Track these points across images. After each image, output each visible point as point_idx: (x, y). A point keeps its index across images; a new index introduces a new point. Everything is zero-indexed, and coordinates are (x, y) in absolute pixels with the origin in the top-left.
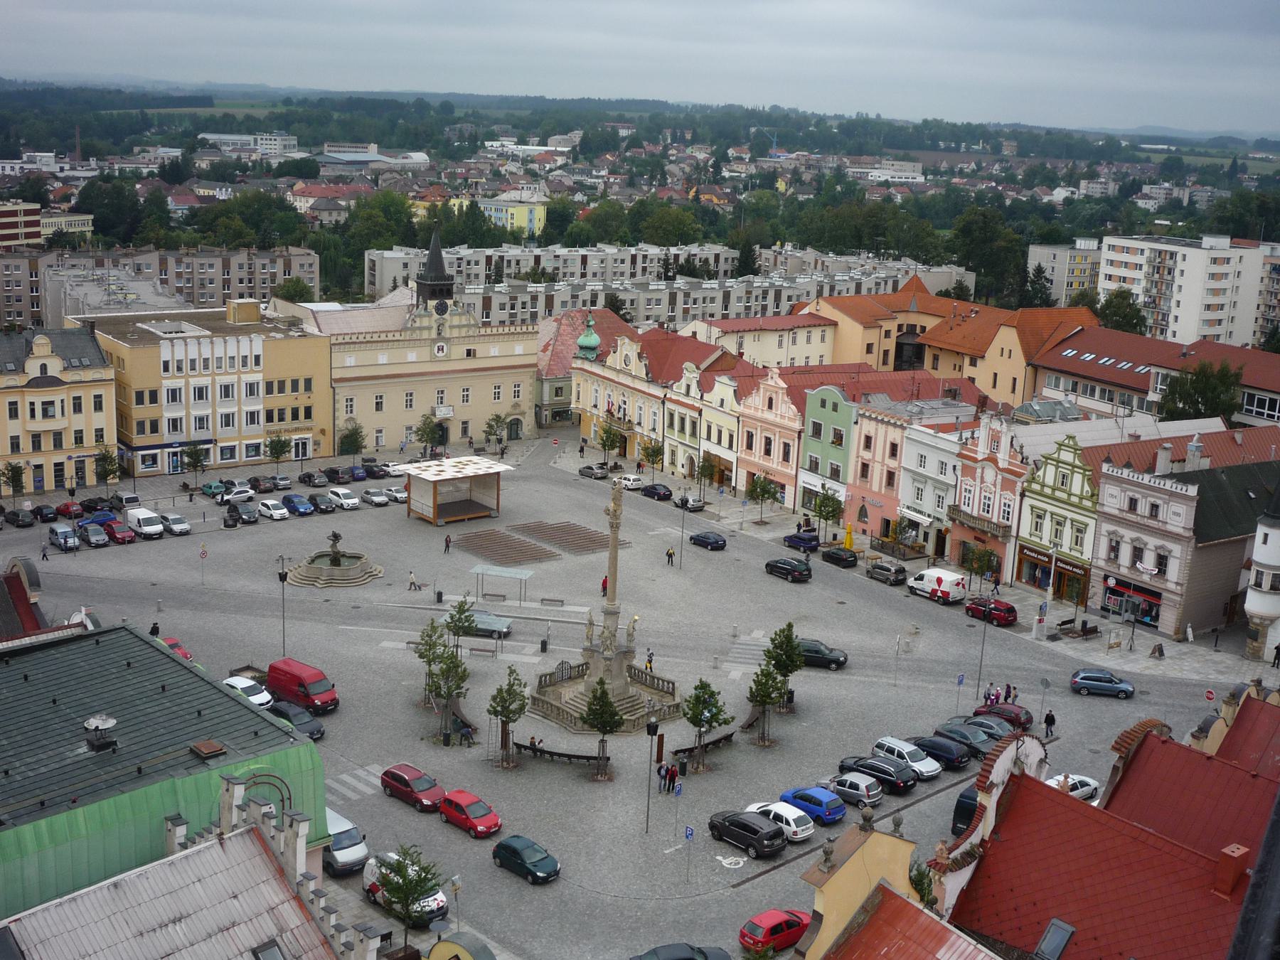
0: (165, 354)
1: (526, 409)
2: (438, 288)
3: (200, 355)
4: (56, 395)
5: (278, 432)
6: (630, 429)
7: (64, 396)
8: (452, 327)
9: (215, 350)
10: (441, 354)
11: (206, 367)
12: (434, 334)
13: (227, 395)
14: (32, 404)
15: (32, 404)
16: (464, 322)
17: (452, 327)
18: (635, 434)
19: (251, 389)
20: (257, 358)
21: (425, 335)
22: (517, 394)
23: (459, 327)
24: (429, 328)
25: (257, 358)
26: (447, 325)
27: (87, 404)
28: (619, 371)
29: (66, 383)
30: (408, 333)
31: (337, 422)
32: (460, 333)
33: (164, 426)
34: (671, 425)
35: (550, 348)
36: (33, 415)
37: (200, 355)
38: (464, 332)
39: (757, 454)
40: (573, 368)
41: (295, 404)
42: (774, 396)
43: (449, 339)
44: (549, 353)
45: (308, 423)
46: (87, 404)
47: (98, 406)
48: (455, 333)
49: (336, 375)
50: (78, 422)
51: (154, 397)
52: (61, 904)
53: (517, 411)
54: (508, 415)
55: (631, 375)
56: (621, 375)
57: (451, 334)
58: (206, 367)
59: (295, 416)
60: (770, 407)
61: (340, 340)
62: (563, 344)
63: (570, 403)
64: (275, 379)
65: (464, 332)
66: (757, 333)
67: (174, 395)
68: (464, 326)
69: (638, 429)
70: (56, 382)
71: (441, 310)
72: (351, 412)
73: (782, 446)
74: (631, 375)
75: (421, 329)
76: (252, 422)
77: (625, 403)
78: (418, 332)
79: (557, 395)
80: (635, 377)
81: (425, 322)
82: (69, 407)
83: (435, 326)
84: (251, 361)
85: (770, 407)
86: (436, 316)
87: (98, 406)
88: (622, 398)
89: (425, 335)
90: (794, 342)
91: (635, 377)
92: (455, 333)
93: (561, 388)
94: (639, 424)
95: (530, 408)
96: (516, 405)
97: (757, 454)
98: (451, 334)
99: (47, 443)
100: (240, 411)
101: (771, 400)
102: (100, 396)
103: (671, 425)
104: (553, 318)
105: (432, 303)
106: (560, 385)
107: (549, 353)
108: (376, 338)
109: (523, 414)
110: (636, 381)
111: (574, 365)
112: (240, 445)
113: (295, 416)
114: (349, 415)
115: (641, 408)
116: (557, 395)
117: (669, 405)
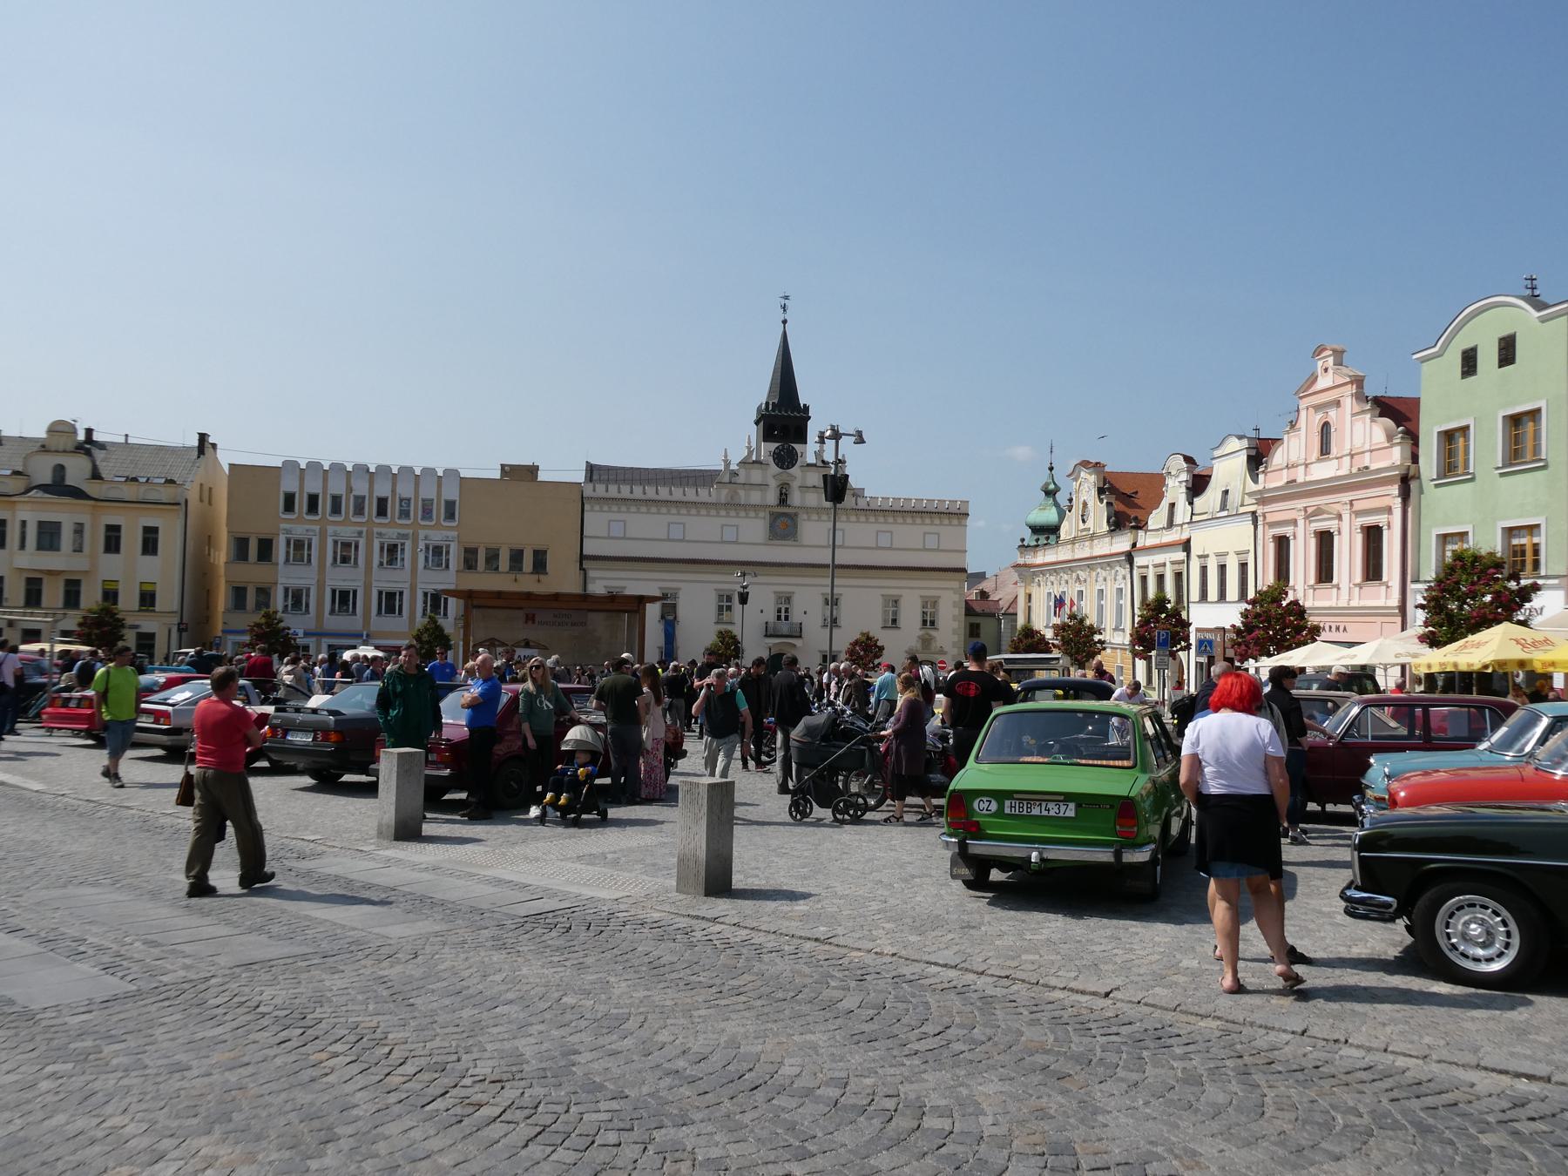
0: (289, 484)
3: (350, 489)
4: (65, 514)
7: (85, 519)
9: (376, 487)
11: (359, 510)
12: (772, 498)
13: (392, 561)
14: (24, 523)
15: (24, 523)
19: (437, 553)
20: (450, 506)
22: (929, 622)
24: (763, 486)
25: (450, 506)
26: (795, 485)
27: (132, 539)
29: (88, 497)
33: (278, 601)
36: (22, 546)
37: (350, 489)
46: (132, 539)
47: (150, 543)
50: (111, 567)
51: (266, 549)
58: (359, 510)
64: (482, 540)
67: (299, 548)
70: (77, 493)
71: (786, 459)
75: (748, 485)
77: (1081, 593)
81: (756, 476)
82: (95, 539)
83: (773, 484)
84: (439, 511)
87: (150, 543)
89: (755, 497)
95: (954, 645)
99: (53, 594)
102: (155, 530)
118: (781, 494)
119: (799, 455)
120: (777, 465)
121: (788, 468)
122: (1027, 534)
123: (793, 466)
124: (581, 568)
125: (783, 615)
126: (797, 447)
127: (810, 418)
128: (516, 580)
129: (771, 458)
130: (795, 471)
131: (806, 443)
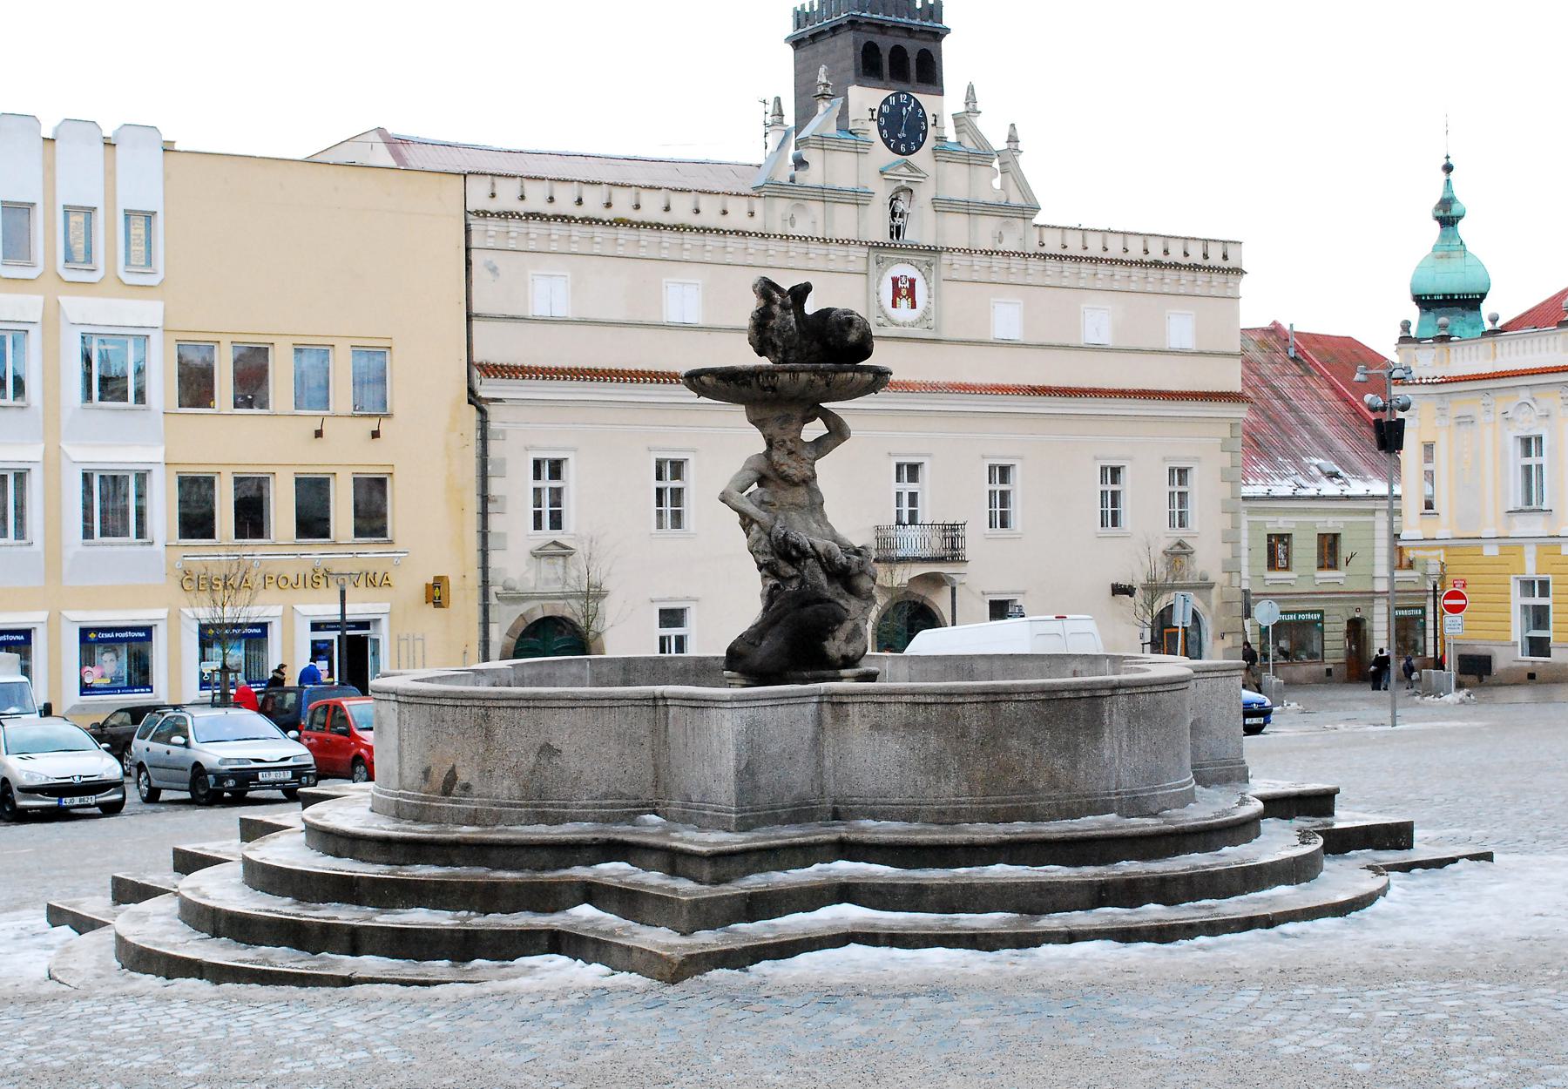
2: (885, 43)
5: (228, 584)
8: (942, 206)
10: (903, 312)
17: (942, 206)
21: (844, 221)
24: (859, 198)
26: (924, 194)
30: (782, 206)
31: (495, 559)
41: (315, 460)
43: (934, 251)
45: (371, 552)
48: (955, 230)
49: (493, 345)
59: (312, 523)
61: (507, 198)
68: (989, 209)
72: (556, 522)
75: (827, 195)
76: (113, 525)
78: (816, 208)
83: (883, 192)
86: (882, 154)
92: (955, 230)
96: (1179, 553)
100: (53, 461)
105: (866, 99)
108: (652, 209)
112: (53, 623)
113: (312, 523)
114: (547, 534)
118: (894, 214)
119: (930, 120)
120: (887, 142)
121: (910, 152)
122: (1413, 313)
123: (919, 145)
124: (473, 397)
125: (906, 508)
126: (925, 100)
127: (948, 30)
128: (319, 434)
129: (874, 126)
130: (922, 158)
131: (941, 93)
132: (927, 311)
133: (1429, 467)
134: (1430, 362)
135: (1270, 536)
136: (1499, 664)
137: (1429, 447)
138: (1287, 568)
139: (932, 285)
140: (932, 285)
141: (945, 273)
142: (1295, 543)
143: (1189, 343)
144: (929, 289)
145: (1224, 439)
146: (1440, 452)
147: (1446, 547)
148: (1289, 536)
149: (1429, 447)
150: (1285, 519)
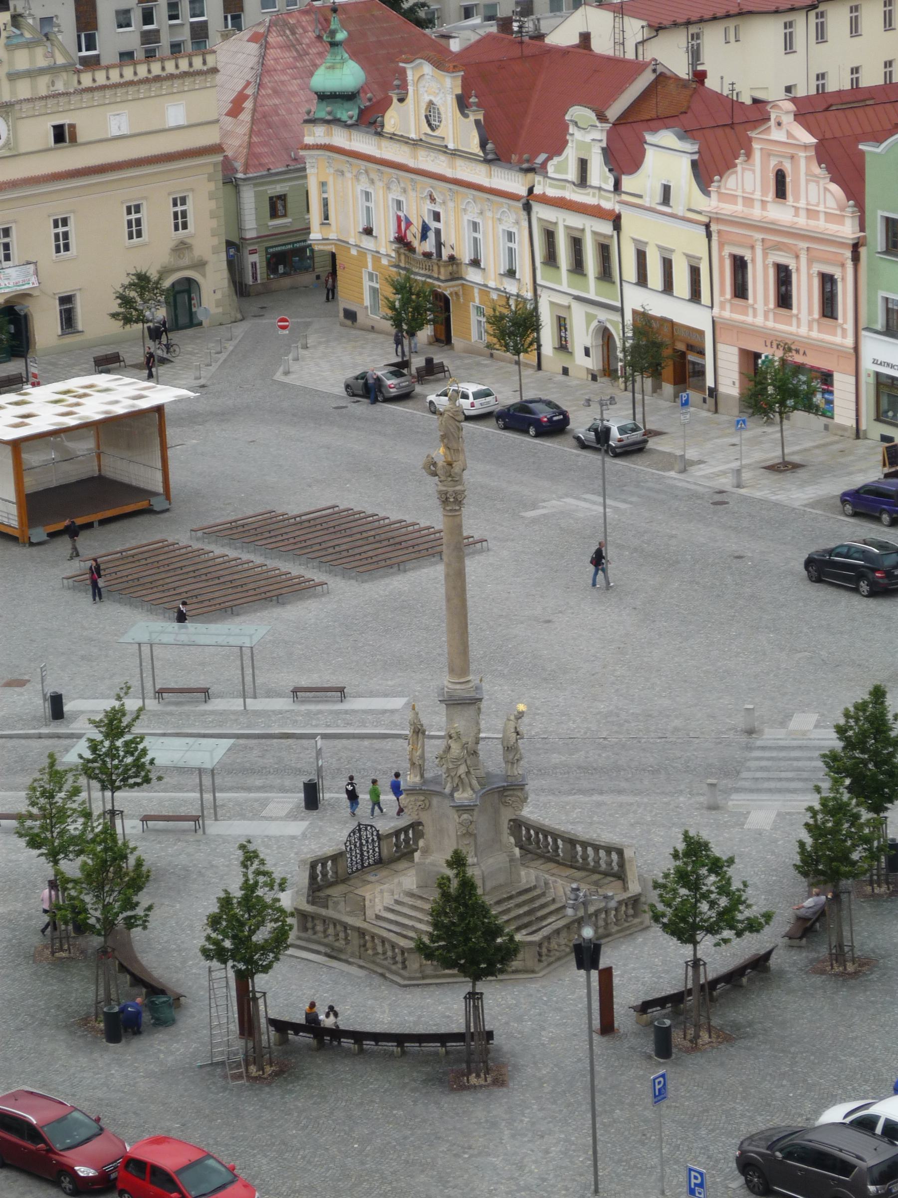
1: (208, 255)
6: (455, 277)
16: (42, 62)
18: (467, 288)
22: (181, 221)
23: (32, 74)
28: (416, 144)
32: (33, 88)
34: (551, 259)
35: (248, 105)
38: (42, 86)
39: (760, 306)
40: (308, 147)
42: (788, 167)
44: (245, 116)
52: (227, 986)
53: (186, 261)
54: (164, 273)
55: (444, 150)
56: (422, 153)
57: (13, 92)
60: (781, 192)
62: (276, 92)
63: (307, 230)
65: (42, 86)
66: (731, 24)
68: (42, 71)
69: (473, 276)
73: (816, 282)
74: (444, 150)
77: (437, 217)
79: (274, 214)
80: (455, 154)
85: (781, 192)
88: (428, 206)
90: (821, 35)
91: (455, 154)
93: (282, 198)
94: (476, 263)
95: (215, 251)
96: (182, 247)
97: (760, 306)
98: (13, 92)
101: (780, 178)
103: (551, 259)
104: (246, 34)
106: (279, 189)
107: (245, 116)
109: (200, 265)
110: (459, 162)
111: (308, 140)
115: (475, 226)
116: (274, 214)
117: (541, 212)
132: (8, 139)
133: (325, 196)
134: (322, 134)
135: (271, 198)
136: (360, 318)
137: (323, 184)
138: (285, 215)
139: (10, 123)
140: (10, 123)
141: (18, 115)
142: (289, 200)
143: (182, 122)
144: (8, 126)
145: (209, 174)
146: (331, 187)
147: (335, 244)
148: (285, 195)
149: (323, 184)
150: (282, 185)
